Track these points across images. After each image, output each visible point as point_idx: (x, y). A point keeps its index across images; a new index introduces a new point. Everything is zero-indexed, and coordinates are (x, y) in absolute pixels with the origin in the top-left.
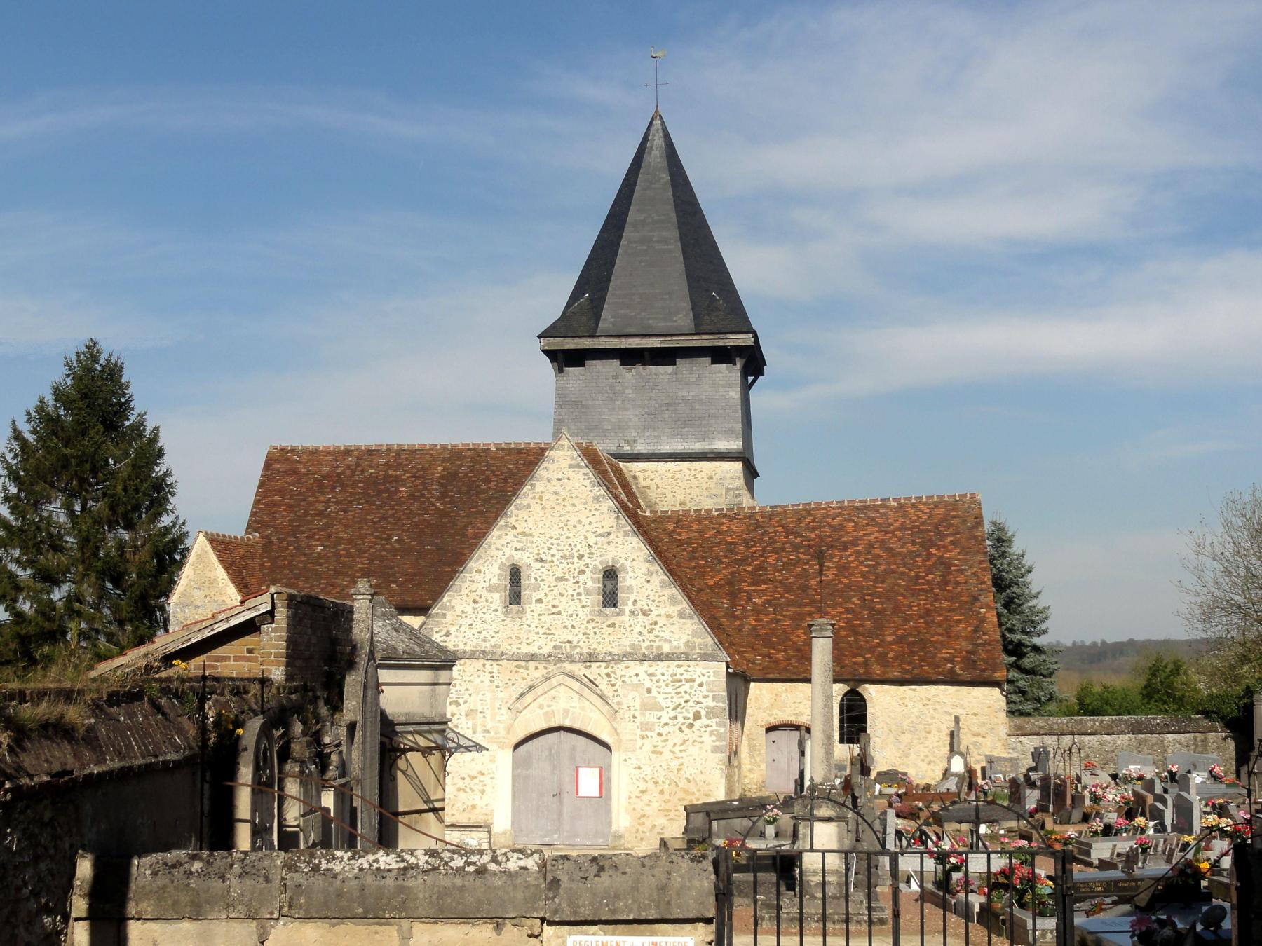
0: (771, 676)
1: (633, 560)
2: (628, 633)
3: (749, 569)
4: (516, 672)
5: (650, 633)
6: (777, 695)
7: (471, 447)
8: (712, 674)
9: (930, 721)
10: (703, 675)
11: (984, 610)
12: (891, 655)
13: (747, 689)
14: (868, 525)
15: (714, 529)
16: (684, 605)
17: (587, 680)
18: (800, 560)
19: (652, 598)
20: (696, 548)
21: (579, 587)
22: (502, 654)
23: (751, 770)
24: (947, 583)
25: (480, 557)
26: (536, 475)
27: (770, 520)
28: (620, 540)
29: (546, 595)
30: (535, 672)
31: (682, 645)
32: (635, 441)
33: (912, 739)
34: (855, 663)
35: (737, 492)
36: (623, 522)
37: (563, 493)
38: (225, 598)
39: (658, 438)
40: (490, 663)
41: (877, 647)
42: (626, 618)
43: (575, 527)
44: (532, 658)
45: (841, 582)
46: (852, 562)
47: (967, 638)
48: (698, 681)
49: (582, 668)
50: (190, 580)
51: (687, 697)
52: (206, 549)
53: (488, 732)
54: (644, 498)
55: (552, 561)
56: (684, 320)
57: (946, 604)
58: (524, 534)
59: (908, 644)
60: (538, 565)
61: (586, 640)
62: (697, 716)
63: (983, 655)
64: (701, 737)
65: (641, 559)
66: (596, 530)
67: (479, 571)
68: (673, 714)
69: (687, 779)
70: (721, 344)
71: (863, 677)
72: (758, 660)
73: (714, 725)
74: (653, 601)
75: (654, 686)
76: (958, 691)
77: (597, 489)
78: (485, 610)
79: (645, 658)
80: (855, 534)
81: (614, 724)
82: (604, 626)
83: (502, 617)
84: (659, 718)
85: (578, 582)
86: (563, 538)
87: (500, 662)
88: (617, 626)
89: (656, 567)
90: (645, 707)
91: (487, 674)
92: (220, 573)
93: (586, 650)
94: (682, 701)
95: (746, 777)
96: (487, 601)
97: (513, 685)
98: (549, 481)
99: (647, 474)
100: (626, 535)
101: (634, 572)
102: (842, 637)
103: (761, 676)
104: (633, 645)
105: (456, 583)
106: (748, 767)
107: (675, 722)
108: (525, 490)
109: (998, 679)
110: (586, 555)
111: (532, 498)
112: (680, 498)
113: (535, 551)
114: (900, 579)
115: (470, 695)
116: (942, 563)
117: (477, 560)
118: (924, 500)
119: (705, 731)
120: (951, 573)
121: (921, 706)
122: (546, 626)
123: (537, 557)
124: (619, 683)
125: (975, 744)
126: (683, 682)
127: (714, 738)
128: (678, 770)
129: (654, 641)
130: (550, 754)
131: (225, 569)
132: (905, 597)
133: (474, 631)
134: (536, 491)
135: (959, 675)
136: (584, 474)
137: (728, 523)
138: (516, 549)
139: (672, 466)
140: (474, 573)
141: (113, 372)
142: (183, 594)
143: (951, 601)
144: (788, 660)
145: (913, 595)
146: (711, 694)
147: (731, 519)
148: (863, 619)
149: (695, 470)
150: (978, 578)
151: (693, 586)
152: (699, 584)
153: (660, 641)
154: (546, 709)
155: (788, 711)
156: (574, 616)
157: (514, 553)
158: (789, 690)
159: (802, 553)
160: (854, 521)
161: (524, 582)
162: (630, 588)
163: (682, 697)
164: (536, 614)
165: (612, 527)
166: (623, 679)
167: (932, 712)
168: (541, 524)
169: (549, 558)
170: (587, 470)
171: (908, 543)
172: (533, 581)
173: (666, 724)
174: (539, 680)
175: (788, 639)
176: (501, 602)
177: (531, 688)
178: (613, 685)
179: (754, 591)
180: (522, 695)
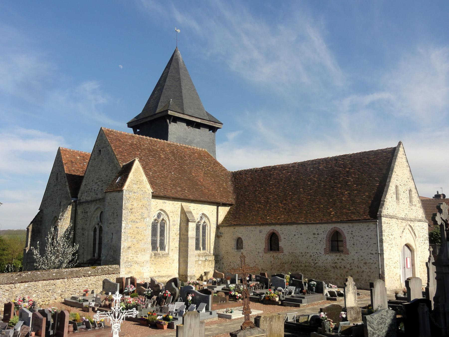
50: (132, 180)
60: (400, 186)
70: (214, 125)
83: (396, 203)
92: (144, 178)
93: (409, 217)
142: (128, 186)
154: (406, 237)
180: (403, 232)
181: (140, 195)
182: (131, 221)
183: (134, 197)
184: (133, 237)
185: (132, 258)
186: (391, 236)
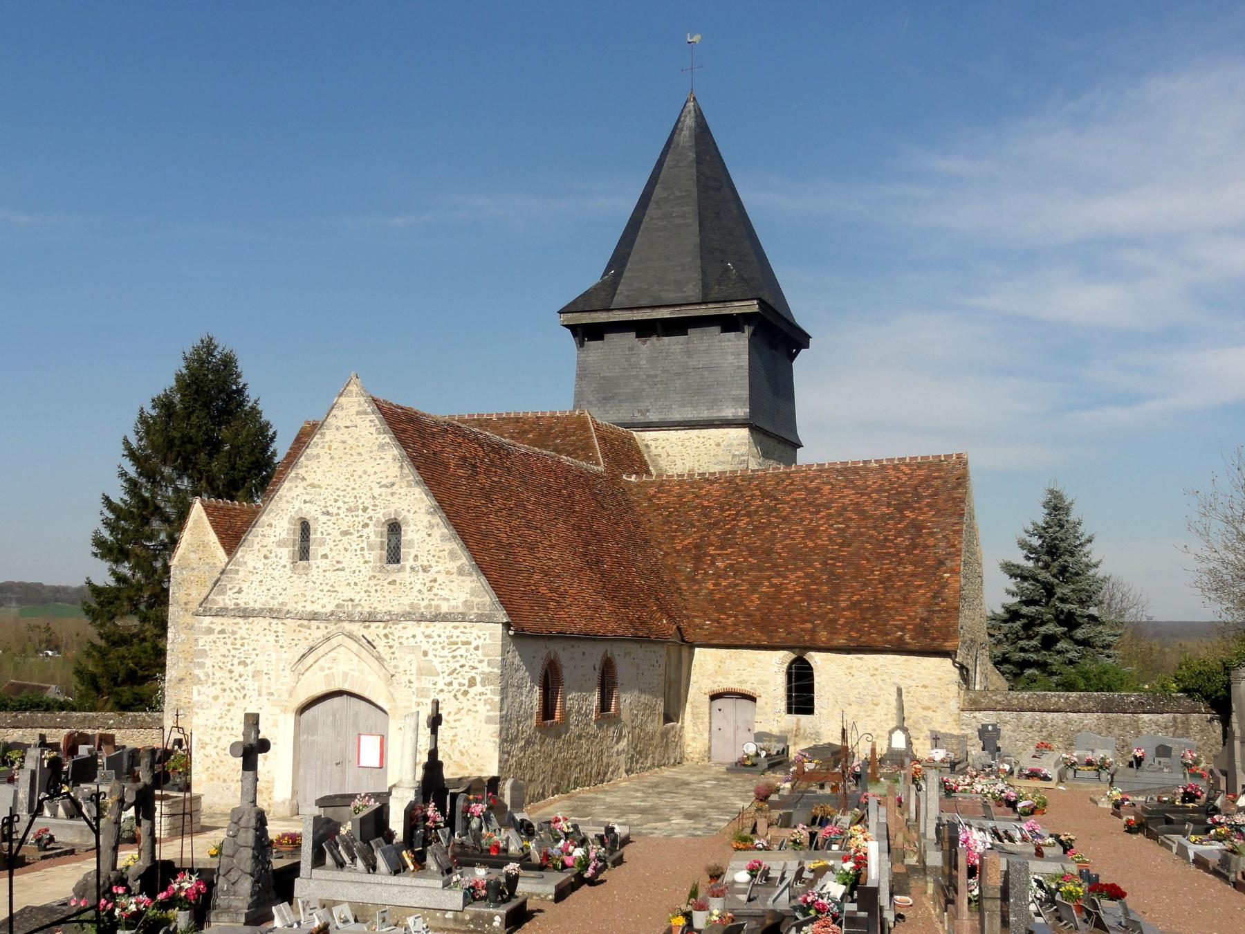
0: (715, 642)
1: (415, 512)
2: (408, 592)
3: (719, 532)
4: (300, 631)
5: (429, 591)
6: (721, 662)
7: (476, 417)
8: (488, 636)
9: (878, 693)
10: (479, 637)
11: (948, 575)
12: (842, 621)
13: (691, 655)
14: (845, 487)
15: (693, 493)
16: (464, 560)
17: (365, 641)
18: (770, 522)
19: (432, 553)
20: (673, 512)
21: (362, 541)
22: (288, 612)
23: (694, 739)
24: (915, 548)
25: (272, 510)
26: (326, 423)
27: (749, 484)
28: (403, 491)
29: (331, 550)
30: (317, 632)
31: (460, 604)
32: (648, 411)
33: (859, 711)
34: (802, 630)
35: (742, 458)
36: (406, 471)
37: (351, 442)
38: (215, 561)
39: (670, 408)
40: (275, 621)
41: (829, 613)
42: (406, 576)
43: (360, 477)
44: (314, 616)
45: (806, 546)
46: (822, 525)
47: (924, 605)
48: (474, 645)
49: (361, 628)
51: (463, 661)
52: (201, 515)
53: (272, 694)
54: (655, 466)
55: (338, 514)
56: (692, 291)
57: (909, 568)
58: (313, 486)
59: (862, 610)
60: (324, 518)
61: (368, 599)
62: (472, 683)
63: (937, 623)
64: (475, 705)
65: (423, 511)
66: (381, 480)
67: (270, 525)
68: (448, 679)
69: (460, 751)
71: (808, 644)
72: (707, 625)
73: (488, 692)
74: (434, 556)
75: (431, 649)
76: (907, 661)
77: (383, 436)
78: (274, 566)
79: (422, 619)
80: (831, 496)
81: (391, 689)
82: (385, 583)
83: (290, 573)
84: (435, 684)
85: (361, 536)
86: (349, 489)
87: (285, 621)
88: (398, 583)
89: (437, 520)
90: (421, 672)
91: (272, 633)
93: (367, 609)
94: (457, 665)
95: (689, 745)
96: (276, 556)
97: (296, 645)
98: (337, 429)
99: (658, 442)
100: (409, 485)
101: (416, 525)
102: (796, 602)
103: (704, 642)
104: (412, 603)
105: (249, 537)
106: (691, 735)
107: (451, 688)
108: (315, 439)
109: (948, 648)
110: (371, 507)
111: (321, 448)
112: (689, 466)
113: (323, 503)
114: (868, 542)
115: (257, 655)
116: (915, 526)
117: (268, 514)
118: (908, 461)
119: (480, 700)
120: (921, 536)
121: (868, 677)
122: (331, 583)
123: (324, 509)
124: (396, 644)
125: (925, 718)
126: (460, 645)
127: (488, 707)
128: (452, 741)
129: (433, 600)
130: (334, 720)
131: (216, 534)
132: (868, 561)
133: (264, 588)
134: (325, 440)
135: (908, 643)
136: (371, 421)
137: (708, 486)
138: (305, 502)
139: (682, 434)
140: (266, 527)
141: (228, 362)
142: (182, 557)
143: (915, 566)
144: (735, 625)
145: (877, 559)
146: (486, 659)
147: (711, 483)
148: (822, 584)
149: (704, 437)
150: (949, 541)
151: (661, 550)
152: (668, 548)
153: (439, 599)
154: (327, 671)
155: (732, 678)
156: (357, 572)
157: (303, 506)
158: (733, 657)
159: (773, 517)
160: (832, 485)
161: (312, 537)
162: (411, 542)
163: (458, 661)
164: (321, 570)
165: (396, 477)
166: (400, 640)
167: (880, 683)
168: (328, 475)
169: (335, 511)
170: (373, 417)
171: (882, 505)
172: (319, 535)
173: (442, 691)
174: (319, 641)
175: (741, 603)
176: (289, 558)
177: (311, 649)
178: (391, 647)
179: (719, 555)
181: (204, 573)
182: (186, 627)
183: (192, 578)
184: (189, 660)
185: (187, 700)
186: (238, 669)
